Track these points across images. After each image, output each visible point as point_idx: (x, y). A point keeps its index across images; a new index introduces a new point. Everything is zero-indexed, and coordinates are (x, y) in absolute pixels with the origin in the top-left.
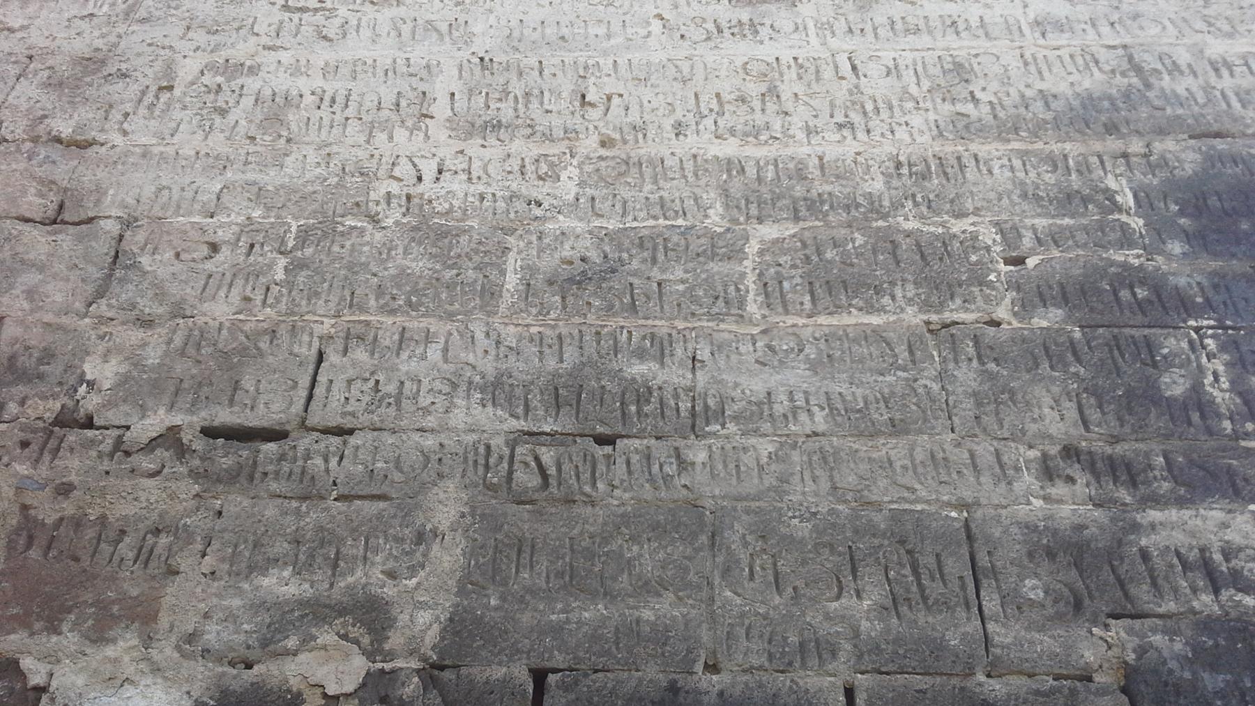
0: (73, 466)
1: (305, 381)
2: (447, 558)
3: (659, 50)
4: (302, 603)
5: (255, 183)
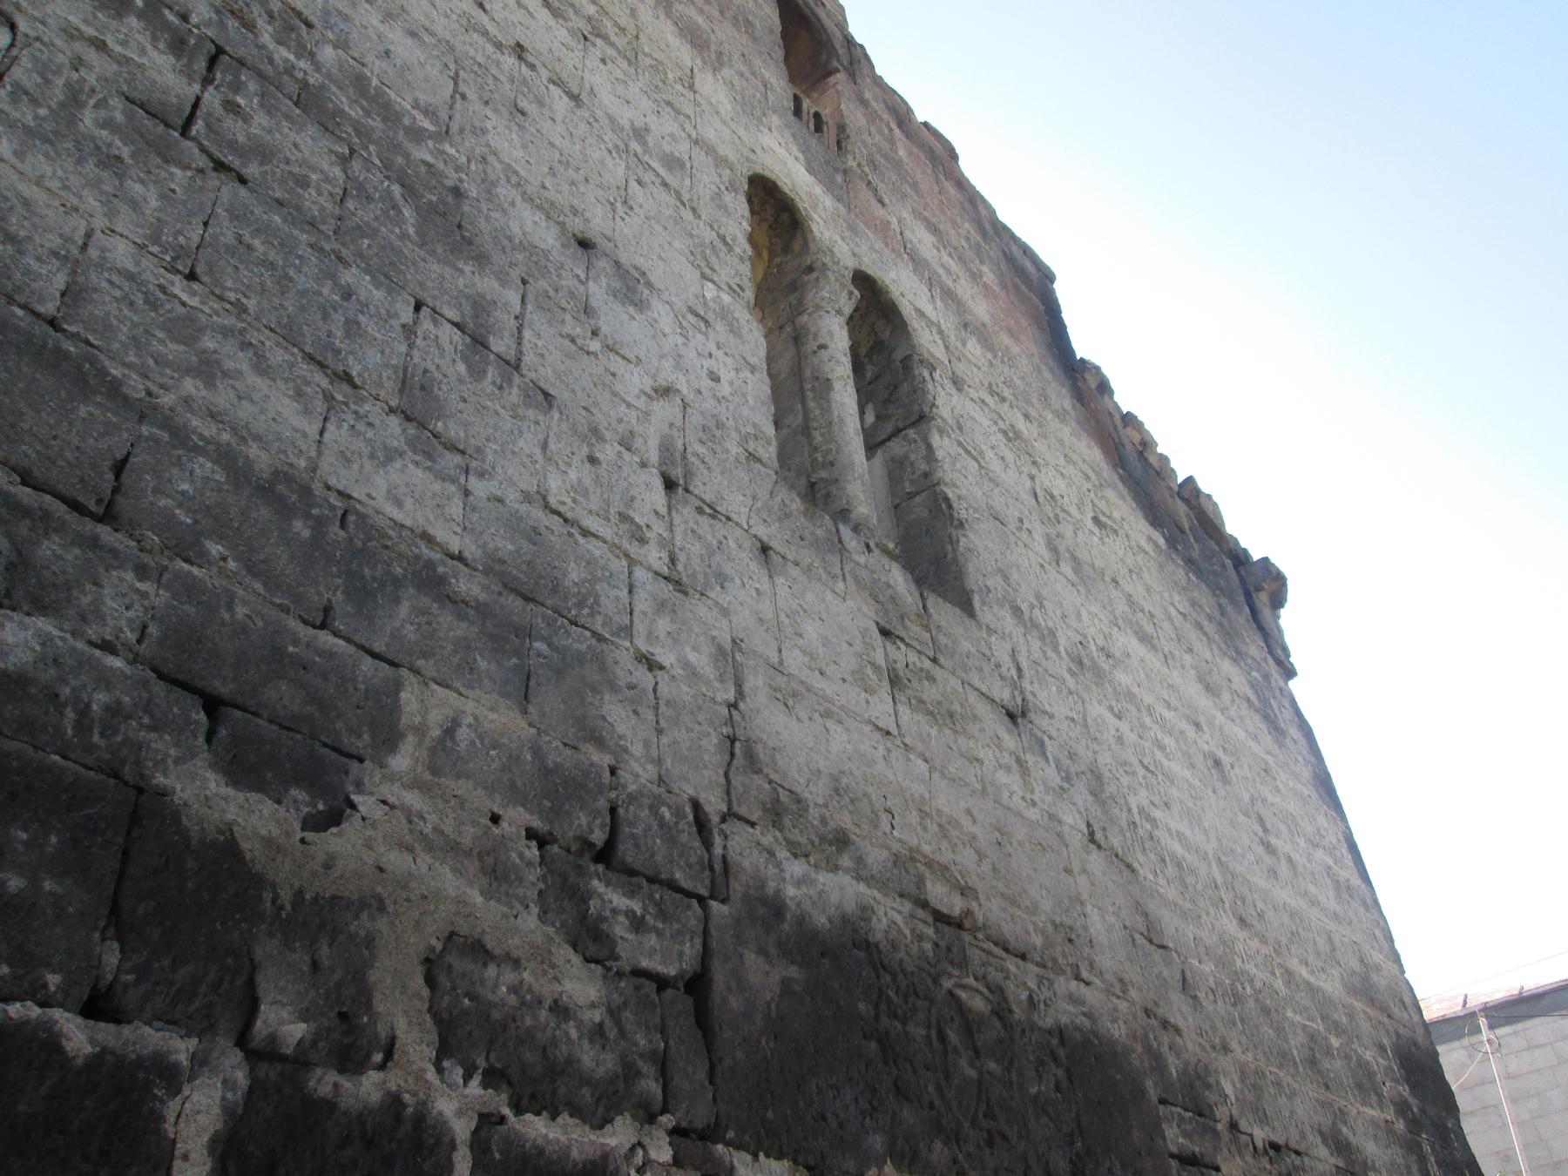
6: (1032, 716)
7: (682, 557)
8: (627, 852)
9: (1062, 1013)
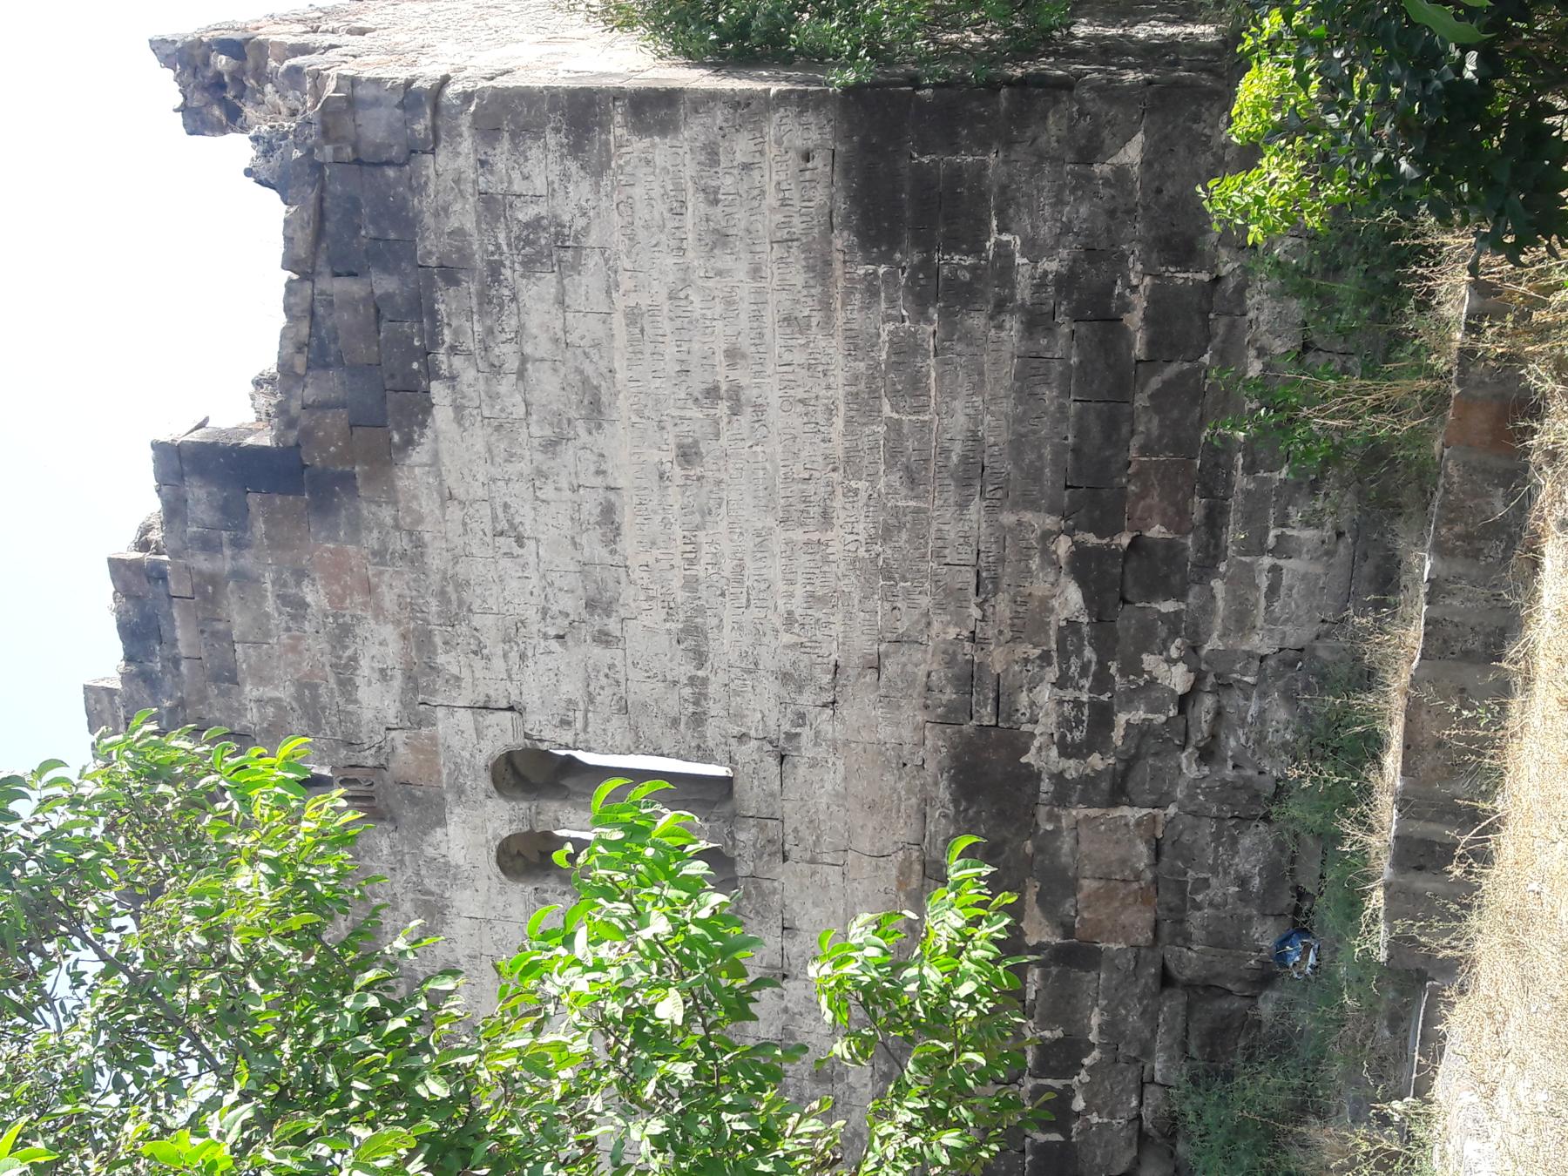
2: (1028, 516)
3: (776, 447)
4: (1041, 556)
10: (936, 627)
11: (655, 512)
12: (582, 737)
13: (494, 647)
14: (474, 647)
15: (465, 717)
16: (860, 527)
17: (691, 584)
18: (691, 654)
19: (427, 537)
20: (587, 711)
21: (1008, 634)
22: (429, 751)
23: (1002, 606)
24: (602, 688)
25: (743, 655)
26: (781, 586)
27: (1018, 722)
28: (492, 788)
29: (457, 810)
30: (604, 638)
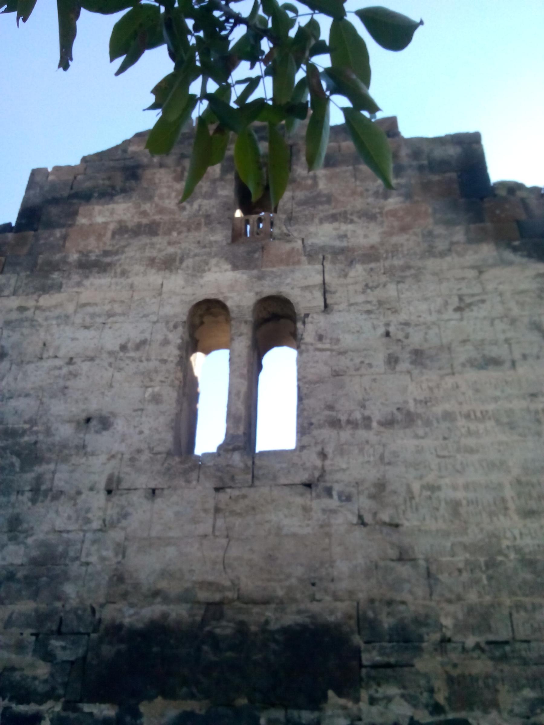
0: (454, 657)
1: (509, 624)
5: (460, 543)
6: (327, 477)
7: (108, 519)
8: (64, 629)
9: (290, 619)
10: (451, 608)
11: (503, 391)
12: (311, 348)
13: (373, 296)
14: (370, 285)
15: (318, 279)
16: (528, 540)
17: (448, 416)
18: (389, 417)
19: (448, 259)
20: (331, 350)
21: (455, 673)
22: (290, 260)
23: (480, 666)
24: (352, 360)
25: (395, 454)
26: (461, 481)
27: (368, 687)
28: (264, 295)
29: (245, 277)
30: (392, 361)
